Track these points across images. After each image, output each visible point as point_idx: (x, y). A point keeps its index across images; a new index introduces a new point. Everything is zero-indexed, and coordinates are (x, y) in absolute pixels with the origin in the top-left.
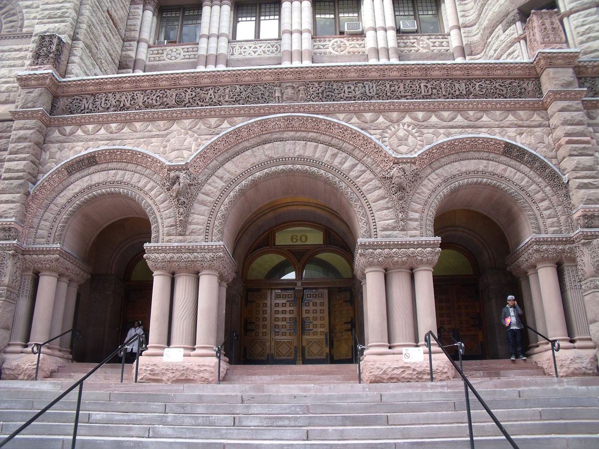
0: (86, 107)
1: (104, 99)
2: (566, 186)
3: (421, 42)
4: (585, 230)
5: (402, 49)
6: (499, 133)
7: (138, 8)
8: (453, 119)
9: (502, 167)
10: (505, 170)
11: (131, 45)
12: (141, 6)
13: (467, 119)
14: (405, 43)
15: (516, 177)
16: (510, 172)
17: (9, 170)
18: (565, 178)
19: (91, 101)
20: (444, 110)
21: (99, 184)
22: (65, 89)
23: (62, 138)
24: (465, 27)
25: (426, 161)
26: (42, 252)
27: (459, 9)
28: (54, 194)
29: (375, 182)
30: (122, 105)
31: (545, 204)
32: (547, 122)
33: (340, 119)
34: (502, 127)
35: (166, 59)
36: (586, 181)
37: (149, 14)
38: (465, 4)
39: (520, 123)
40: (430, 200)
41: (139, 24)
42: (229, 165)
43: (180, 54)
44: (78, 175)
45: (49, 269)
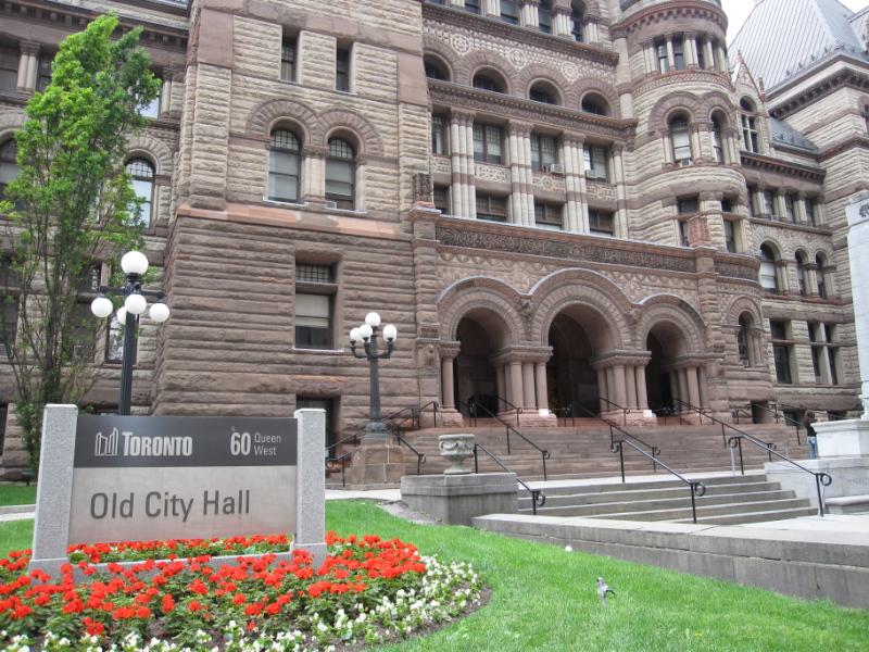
15: (683, 320)
16: (680, 317)
17: (423, 286)
23: (444, 262)
27: (625, 168)
29: (620, 317)
33: (602, 274)
42: (549, 297)
44: (461, 293)
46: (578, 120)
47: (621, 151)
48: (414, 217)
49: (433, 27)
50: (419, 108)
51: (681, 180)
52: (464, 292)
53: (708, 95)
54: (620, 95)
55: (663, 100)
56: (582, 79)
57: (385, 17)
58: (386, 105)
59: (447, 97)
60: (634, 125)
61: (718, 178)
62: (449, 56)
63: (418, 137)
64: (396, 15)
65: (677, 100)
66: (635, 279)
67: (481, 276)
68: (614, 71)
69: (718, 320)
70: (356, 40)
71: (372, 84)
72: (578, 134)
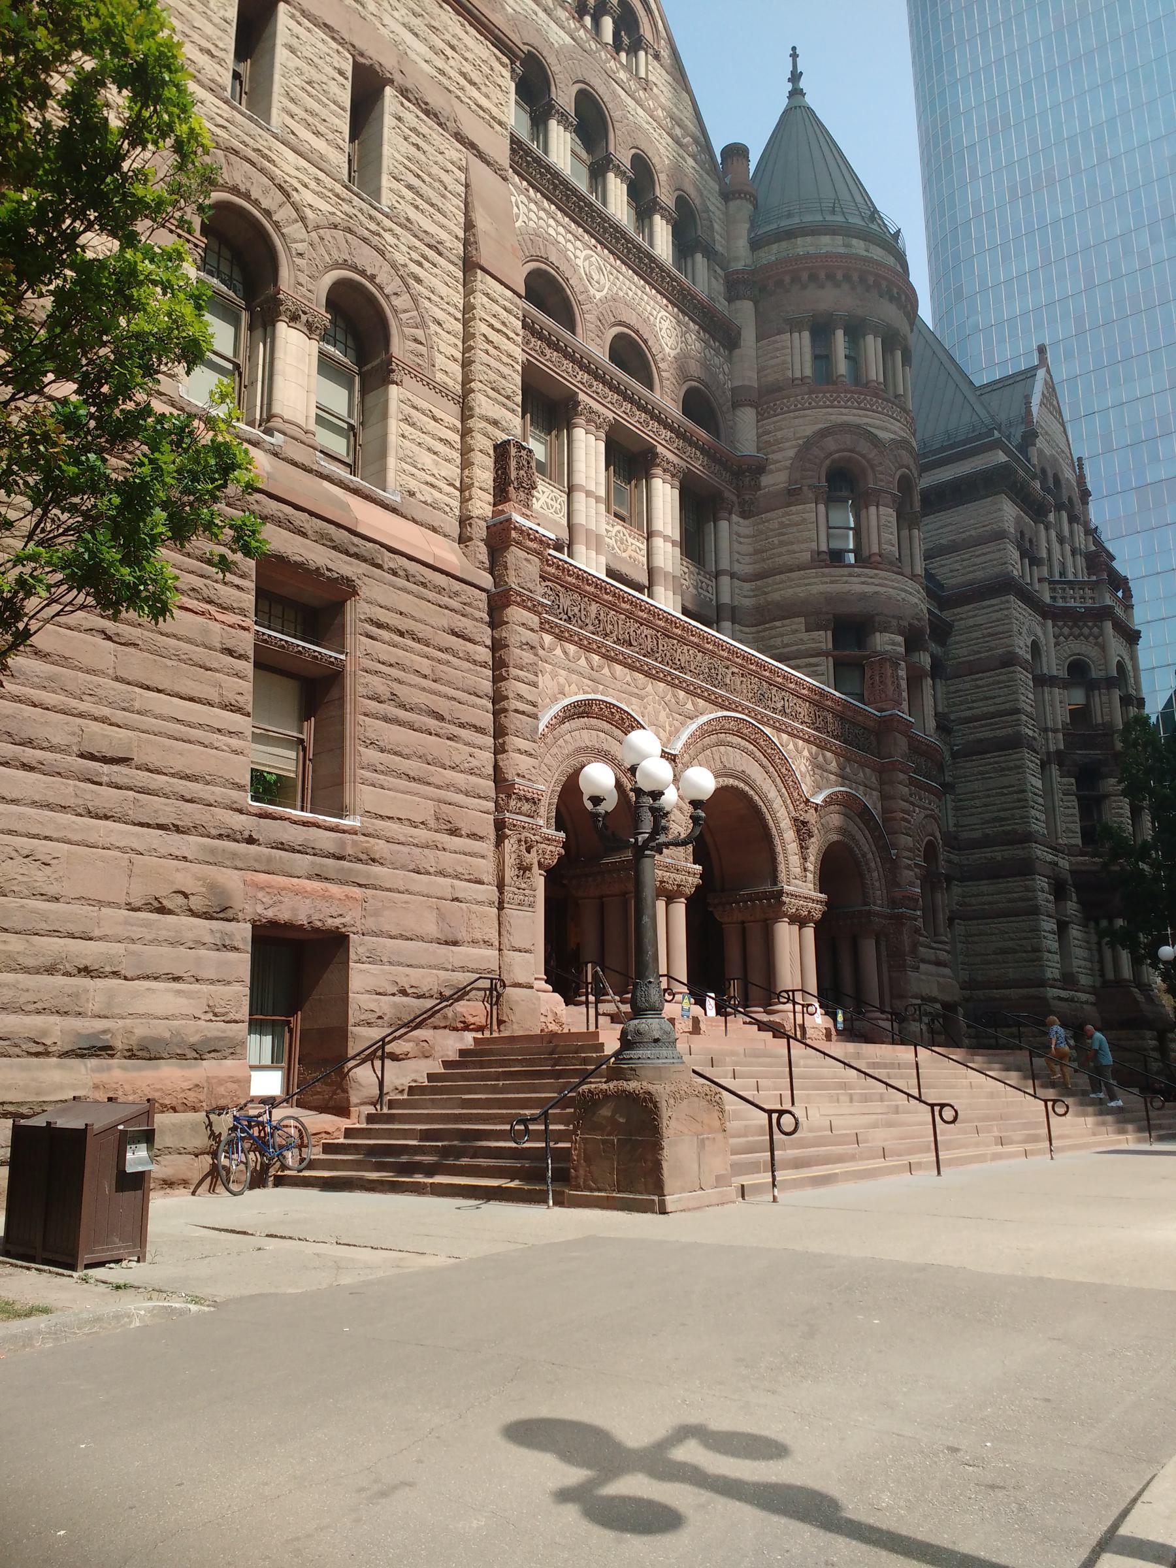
47: (730, 514)
51: (847, 587)
55: (823, 434)
60: (759, 468)
61: (903, 595)
63: (505, 359)
66: (806, 753)
70: (391, 82)
71: (419, 202)
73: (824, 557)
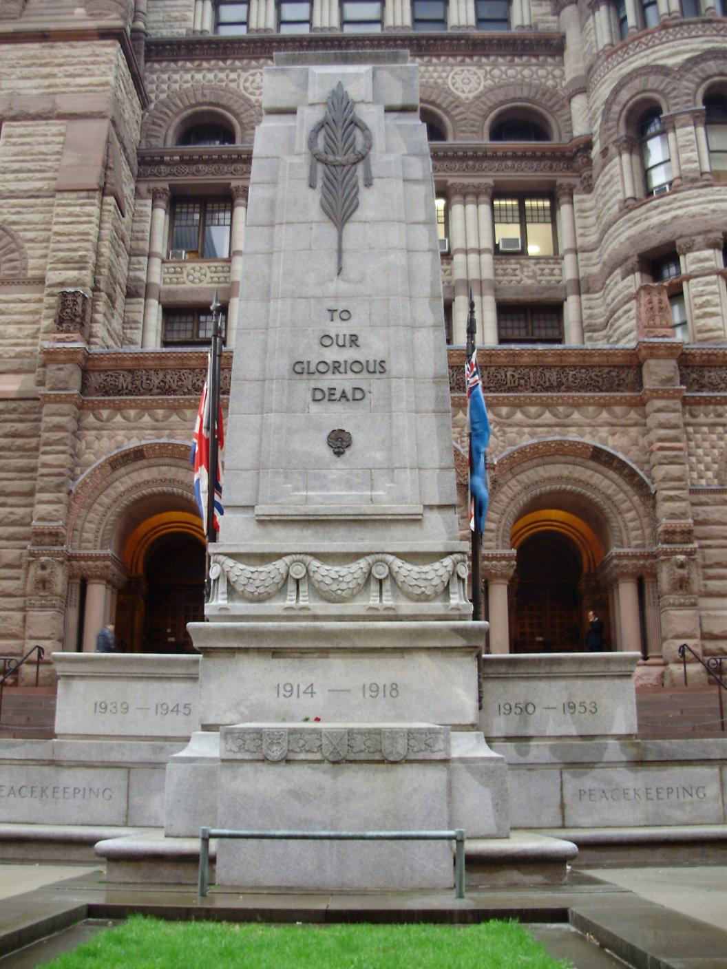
0: (125, 386)
1: (145, 378)
2: (654, 496)
3: (525, 269)
4: (665, 546)
5: (500, 278)
6: (590, 433)
7: (145, 205)
8: (540, 416)
9: (589, 473)
10: (591, 477)
11: (139, 263)
12: (149, 202)
13: (555, 415)
14: (505, 270)
15: (603, 483)
18: (653, 488)
19: (129, 380)
20: (531, 404)
21: (148, 482)
22: (96, 362)
23: (98, 424)
24: (584, 251)
25: (506, 466)
26: (90, 558)
27: (578, 222)
28: (97, 492)
30: (167, 387)
31: (632, 514)
32: (642, 421)
34: (593, 426)
35: (187, 281)
36: (672, 493)
37: (161, 215)
38: (586, 217)
39: (614, 421)
40: (508, 509)
41: (149, 229)
43: (205, 275)
44: (123, 470)
45: (100, 577)
46: (475, 157)
48: (50, 357)
49: (210, 70)
50: (84, 194)
52: (129, 468)
53: (694, 61)
54: (570, 101)
55: (616, 92)
56: (490, 90)
57: (54, 76)
58: (38, 201)
59: (226, 168)
60: (588, 145)
61: (712, 206)
62: (235, 107)
64: (71, 69)
65: (637, 84)
67: (164, 440)
68: (562, 63)
69: (680, 479)
71: (20, 176)
72: (476, 181)
73: (631, 202)
